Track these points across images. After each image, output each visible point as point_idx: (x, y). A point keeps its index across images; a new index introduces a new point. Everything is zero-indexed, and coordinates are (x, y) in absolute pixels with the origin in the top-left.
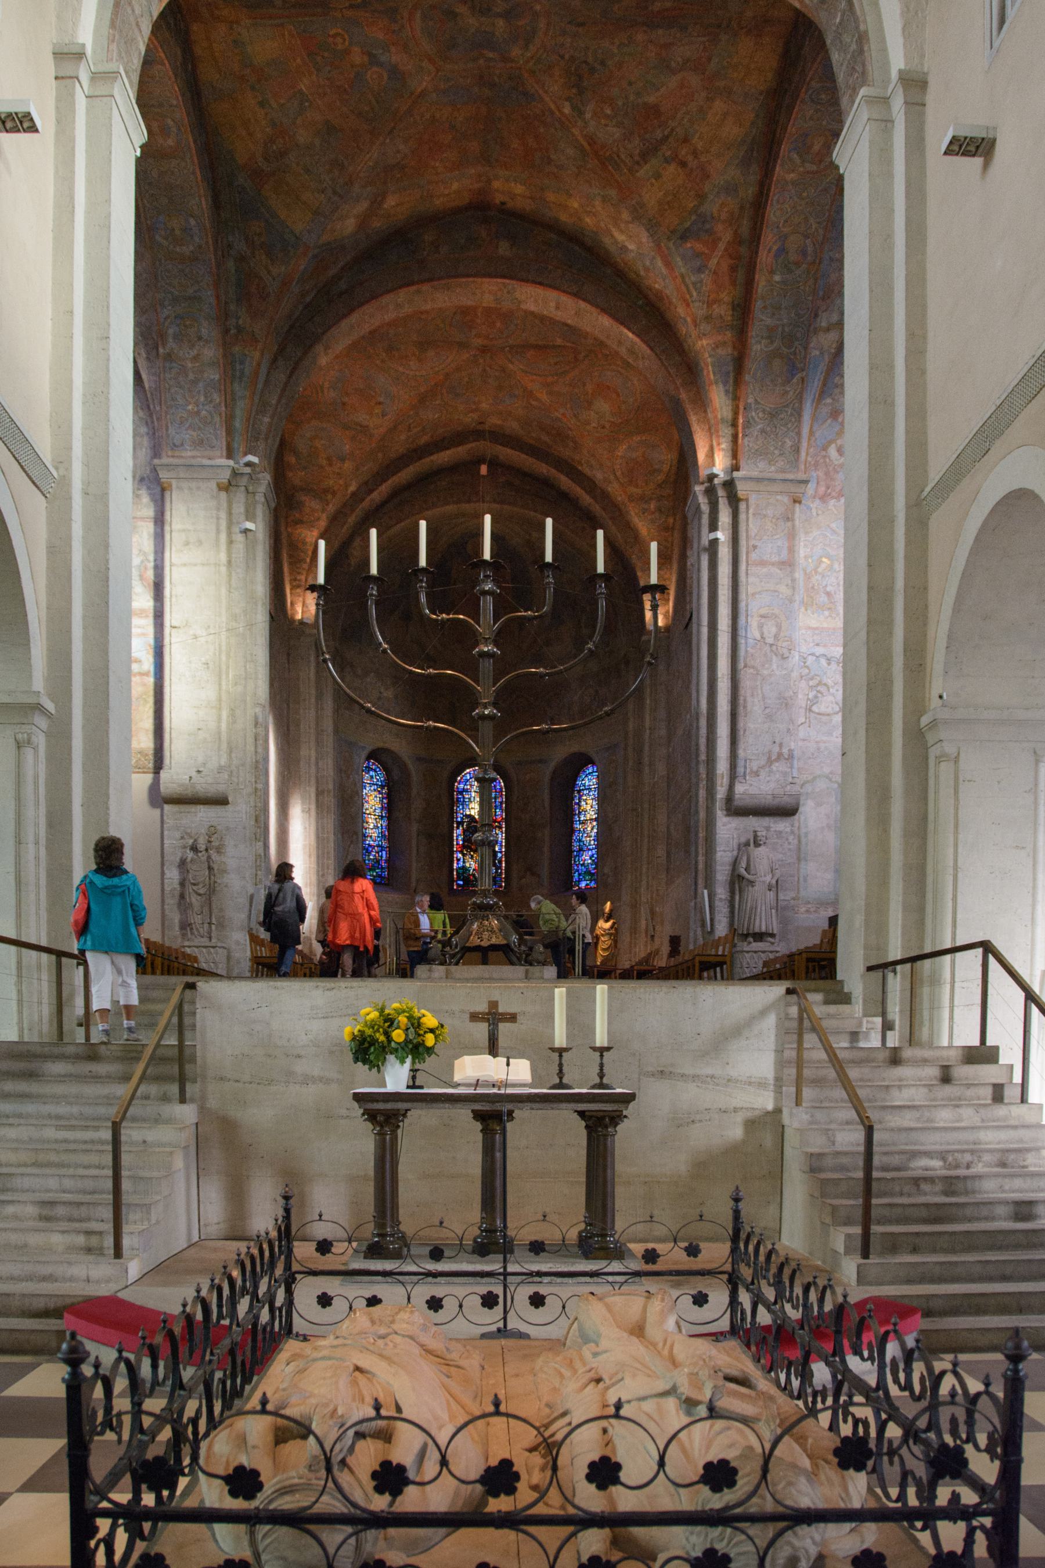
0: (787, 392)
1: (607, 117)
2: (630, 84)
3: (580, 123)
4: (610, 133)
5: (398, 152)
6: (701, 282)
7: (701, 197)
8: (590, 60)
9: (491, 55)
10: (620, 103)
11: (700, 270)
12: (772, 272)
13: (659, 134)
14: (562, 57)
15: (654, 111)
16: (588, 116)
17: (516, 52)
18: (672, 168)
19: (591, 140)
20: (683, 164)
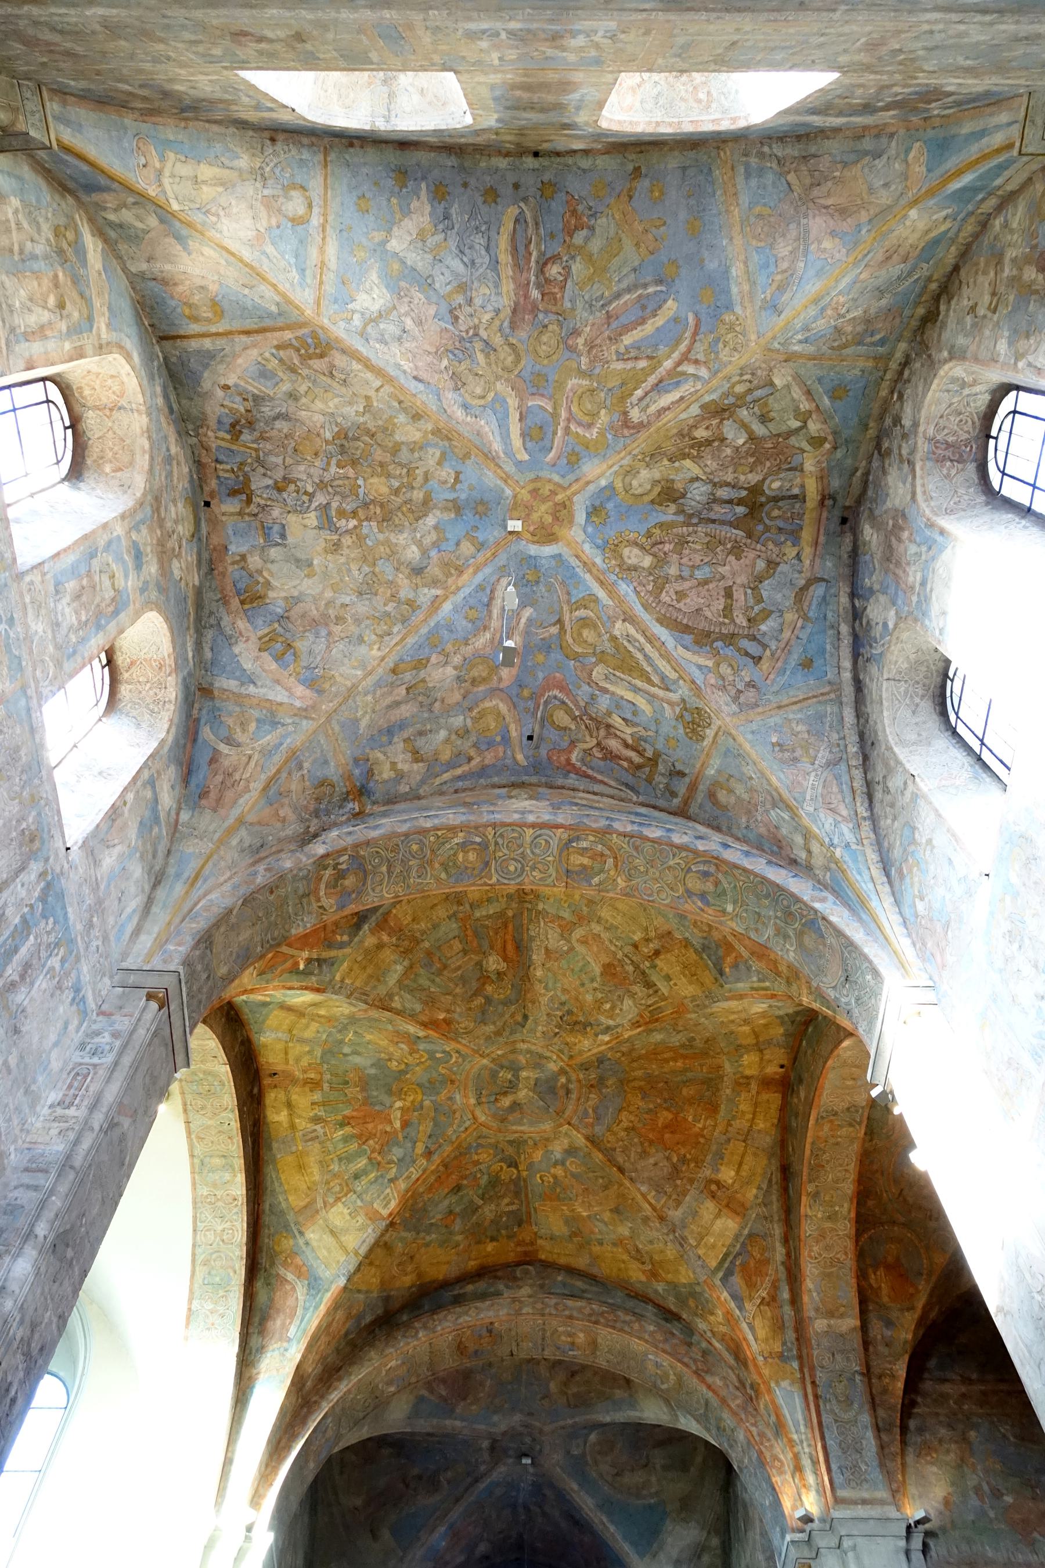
0: (831, 947)
1: (613, 1008)
2: (583, 985)
3: (619, 1030)
4: (629, 1009)
5: (656, 1164)
6: (759, 972)
7: (687, 944)
8: (559, 1013)
9: (563, 1080)
10: (600, 995)
11: (749, 968)
12: (724, 912)
13: (631, 969)
14: (556, 1034)
15: (609, 970)
16: (611, 1023)
17: (553, 1067)
18: (658, 962)
19: (636, 1024)
20: (657, 953)
